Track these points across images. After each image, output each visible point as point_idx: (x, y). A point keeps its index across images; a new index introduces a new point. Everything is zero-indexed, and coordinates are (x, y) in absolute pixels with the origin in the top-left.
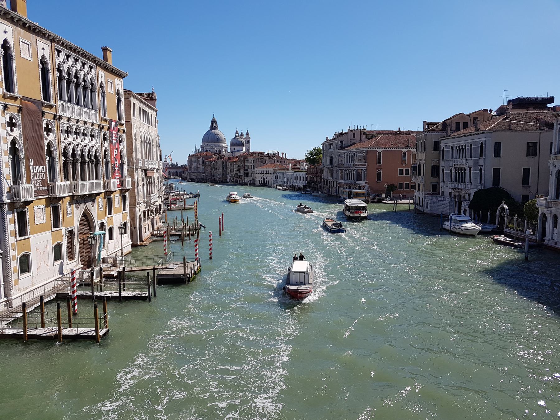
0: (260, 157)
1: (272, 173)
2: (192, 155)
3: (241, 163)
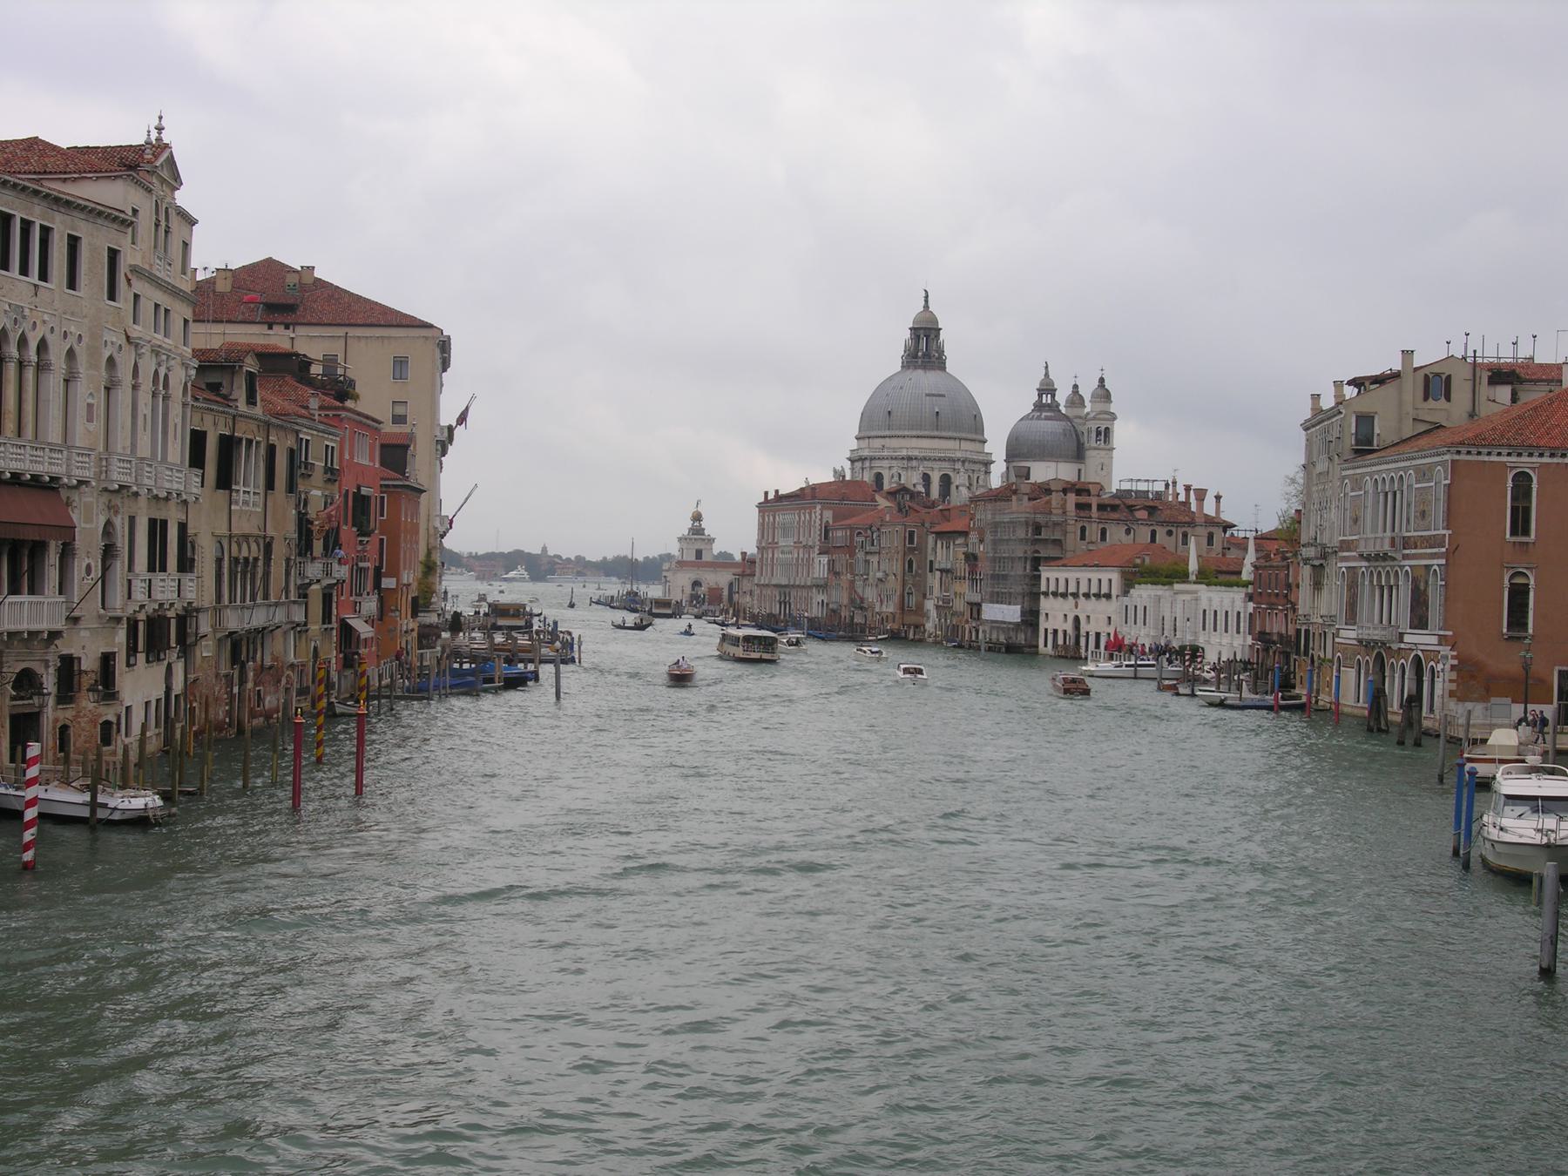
0: (1071, 507)
1: (1114, 593)
2: (779, 498)
3: (981, 541)
